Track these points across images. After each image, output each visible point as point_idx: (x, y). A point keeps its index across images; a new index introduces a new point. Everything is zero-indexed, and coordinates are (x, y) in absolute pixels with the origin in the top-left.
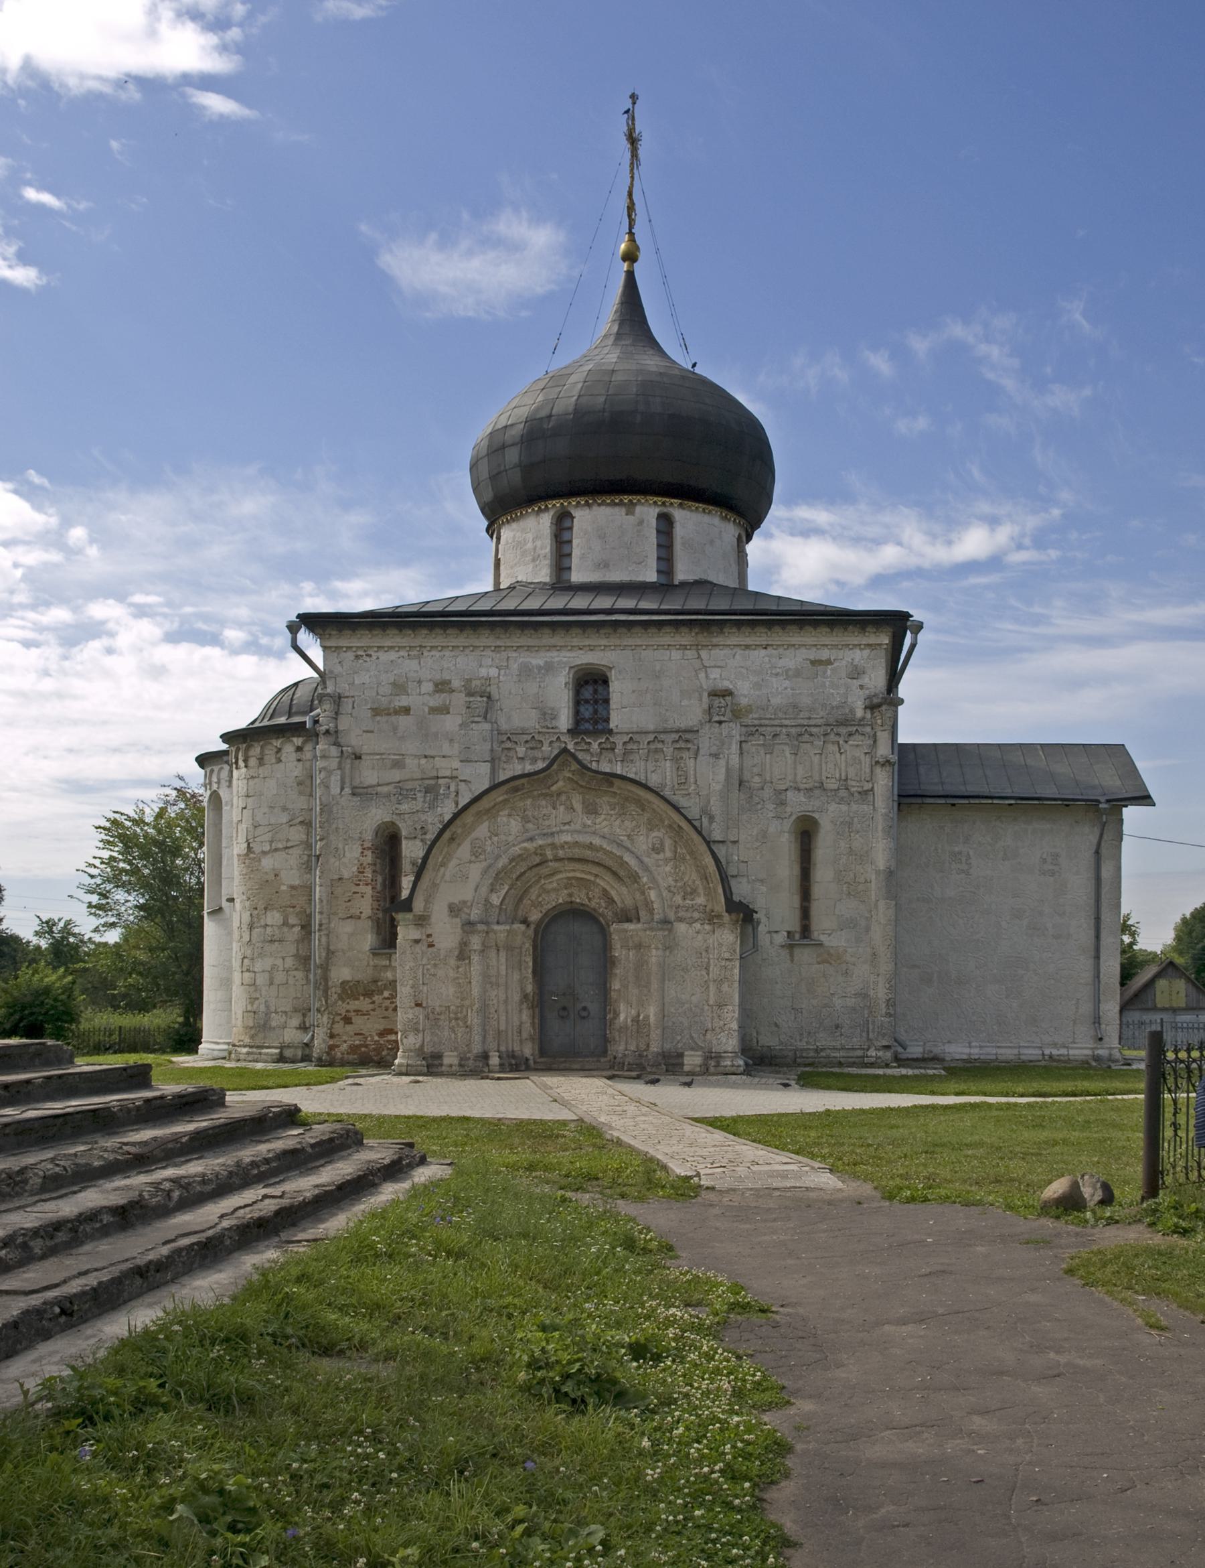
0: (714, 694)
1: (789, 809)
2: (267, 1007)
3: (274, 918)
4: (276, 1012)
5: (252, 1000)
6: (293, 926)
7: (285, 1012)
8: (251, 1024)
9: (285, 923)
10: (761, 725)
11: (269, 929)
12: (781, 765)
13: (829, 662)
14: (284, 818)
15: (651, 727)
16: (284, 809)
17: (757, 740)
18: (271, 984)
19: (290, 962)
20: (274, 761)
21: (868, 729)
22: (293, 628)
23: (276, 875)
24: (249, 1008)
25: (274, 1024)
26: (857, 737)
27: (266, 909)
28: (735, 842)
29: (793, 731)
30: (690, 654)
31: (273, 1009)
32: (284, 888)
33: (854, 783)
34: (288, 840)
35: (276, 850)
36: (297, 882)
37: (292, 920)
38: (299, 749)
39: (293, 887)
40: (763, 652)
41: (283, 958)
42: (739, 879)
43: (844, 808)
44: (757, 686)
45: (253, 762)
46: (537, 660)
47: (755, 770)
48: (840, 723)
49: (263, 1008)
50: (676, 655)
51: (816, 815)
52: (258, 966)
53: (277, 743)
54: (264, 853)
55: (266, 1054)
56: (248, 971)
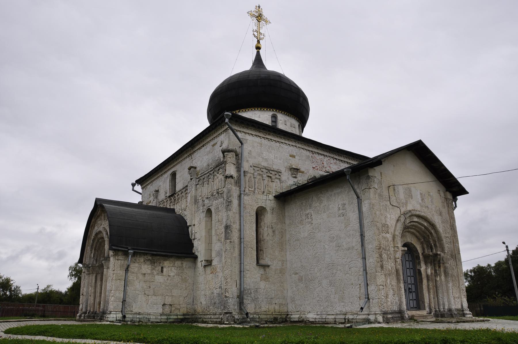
0: (189, 169)
1: (205, 207)
10: (201, 176)
12: (205, 190)
13: (216, 143)
15: (182, 188)
17: (200, 183)
21: (223, 165)
22: (133, 185)
26: (221, 170)
28: (194, 225)
29: (208, 175)
30: (190, 157)
33: (220, 190)
40: (203, 148)
42: (196, 240)
43: (217, 201)
44: (201, 161)
46: (166, 176)
47: (200, 194)
48: (217, 166)
50: (188, 159)
51: (210, 208)
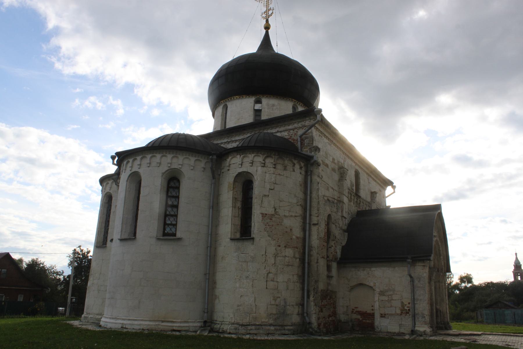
2: (285, 302)
3: (289, 252)
4: (289, 306)
5: (275, 299)
6: (296, 258)
7: (293, 305)
8: (274, 312)
9: (294, 257)
11: (287, 259)
14: (295, 201)
16: (295, 196)
18: (288, 289)
19: (295, 277)
20: (292, 170)
23: (291, 230)
24: (273, 302)
25: (288, 312)
27: (285, 247)
31: (288, 304)
32: (294, 237)
34: (296, 213)
35: (291, 216)
36: (298, 236)
37: (297, 256)
38: (301, 168)
39: (297, 238)
41: (293, 275)
45: (279, 167)
49: (282, 303)
52: (281, 278)
53: (296, 162)
54: (285, 216)
55: (289, 330)
56: (273, 280)
